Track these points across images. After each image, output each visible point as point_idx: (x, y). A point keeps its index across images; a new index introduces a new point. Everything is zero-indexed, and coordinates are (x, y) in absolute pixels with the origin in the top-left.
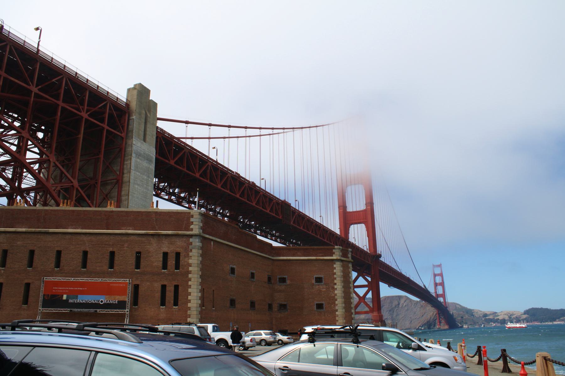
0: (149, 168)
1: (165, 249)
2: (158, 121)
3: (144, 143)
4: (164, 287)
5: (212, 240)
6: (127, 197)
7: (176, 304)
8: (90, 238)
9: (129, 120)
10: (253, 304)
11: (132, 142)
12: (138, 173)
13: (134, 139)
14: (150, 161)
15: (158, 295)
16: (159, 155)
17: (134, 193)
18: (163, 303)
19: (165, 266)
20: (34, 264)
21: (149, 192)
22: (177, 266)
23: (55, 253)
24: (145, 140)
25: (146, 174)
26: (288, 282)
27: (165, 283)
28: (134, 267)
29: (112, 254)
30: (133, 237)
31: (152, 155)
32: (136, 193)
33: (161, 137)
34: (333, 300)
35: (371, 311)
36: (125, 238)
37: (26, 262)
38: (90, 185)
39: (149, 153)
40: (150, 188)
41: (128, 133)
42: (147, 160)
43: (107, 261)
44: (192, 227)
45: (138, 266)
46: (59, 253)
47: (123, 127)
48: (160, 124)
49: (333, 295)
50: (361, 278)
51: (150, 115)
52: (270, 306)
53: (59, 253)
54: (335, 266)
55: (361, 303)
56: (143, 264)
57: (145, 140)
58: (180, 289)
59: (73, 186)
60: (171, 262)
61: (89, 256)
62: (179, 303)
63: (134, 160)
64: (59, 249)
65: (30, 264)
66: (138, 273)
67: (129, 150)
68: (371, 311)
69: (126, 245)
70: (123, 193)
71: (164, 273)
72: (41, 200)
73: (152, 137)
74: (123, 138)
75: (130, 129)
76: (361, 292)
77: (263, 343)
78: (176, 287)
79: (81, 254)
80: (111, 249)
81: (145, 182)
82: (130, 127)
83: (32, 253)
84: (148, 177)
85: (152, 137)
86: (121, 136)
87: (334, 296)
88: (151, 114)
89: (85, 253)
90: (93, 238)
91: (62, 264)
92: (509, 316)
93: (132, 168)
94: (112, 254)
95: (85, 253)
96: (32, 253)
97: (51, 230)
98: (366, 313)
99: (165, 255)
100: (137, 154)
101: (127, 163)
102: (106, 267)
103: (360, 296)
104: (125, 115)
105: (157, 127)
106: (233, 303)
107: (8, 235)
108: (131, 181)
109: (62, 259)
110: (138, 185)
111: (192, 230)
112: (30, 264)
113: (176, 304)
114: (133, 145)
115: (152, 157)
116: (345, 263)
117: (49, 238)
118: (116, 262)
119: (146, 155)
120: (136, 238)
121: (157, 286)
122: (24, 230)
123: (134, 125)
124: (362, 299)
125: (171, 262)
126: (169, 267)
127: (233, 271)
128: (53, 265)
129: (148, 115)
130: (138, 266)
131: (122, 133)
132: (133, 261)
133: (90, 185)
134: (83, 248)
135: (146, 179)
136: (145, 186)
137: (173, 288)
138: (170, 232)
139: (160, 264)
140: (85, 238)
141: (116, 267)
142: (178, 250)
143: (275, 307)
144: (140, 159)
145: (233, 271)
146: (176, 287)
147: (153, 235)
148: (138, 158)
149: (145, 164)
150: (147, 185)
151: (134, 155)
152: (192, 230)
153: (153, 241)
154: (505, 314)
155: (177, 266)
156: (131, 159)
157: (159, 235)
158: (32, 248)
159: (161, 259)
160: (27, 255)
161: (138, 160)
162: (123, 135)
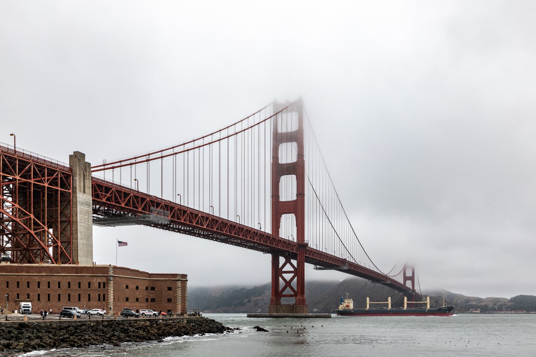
0: (89, 210)
1: (99, 281)
2: (93, 173)
3: (84, 194)
4: (99, 295)
5: (117, 277)
6: (76, 231)
7: (104, 301)
8: (70, 277)
9: (73, 180)
10: (137, 300)
11: (77, 196)
12: (82, 215)
13: (77, 193)
14: (89, 205)
15: (97, 298)
16: (95, 198)
17: (81, 229)
18: (99, 300)
19: (99, 287)
20: (50, 287)
21: (90, 226)
22: (104, 288)
23: (58, 283)
24: (84, 192)
25: (87, 215)
26: (156, 289)
27: (100, 293)
28: (88, 288)
29: (79, 283)
30: (86, 277)
31: (90, 201)
32: (82, 228)
33: (95, 184)
34: (176, 297)
35: (295, 295)
36: (84, 277)
37: (47, 286)
38: (51, 222)
39: (88, 201)
40: (90, 223)
41: (74, 192)
42: (87, 205)
43: (78, 286)
44: (109, 273)
45: (89, 287)
46: (59, 283)
47: (69, 185)
48: (94, 174)
49: (176, 295)
50: (288, 264)
51: (87, 173)
52: (147, 300)
53: (59, 283)
54: (177, 283)
55: (287, 287)
56: (91, 286)
57: (84, 192)
58: (105, 296)
59: (45, 230)
60: (102, 286)
61: (71, 284)
62: (105, 300)
63: (79, 208)
64: (59, 281)
65: (49, 287)
66: (90, 290)
67: (74, 200)
68: (295, 295)
69: (84, 280)
70: (74, 229)
71: (99, 290)
72: (24, 237)
73: (89, 189)
74: (70, 193)
75: (74, 186)
76: (288, 277)
77: (134, 316)
78: (104, 295)
79: (68, 283)
80: (79, 281)
81: (87, 220)
82: (74, 185)
83: (49, 283)
84: (89, 216)
85: (89, 189)
86: (69, 192)
87: (176, 296)
88: (87, 172)
89: (69, 283)
90: (72, 277)
91: (61, 287)
92: (493, 303)
93: (78, 213)
94: (79, 283)
95: (69, 283)
96: (49, 283)
97: (55, 274)
98: (291, 296)
99: (99, 283)
100: (80, 203)
101: (74, 209)
102: (77, 288)
103: (287, 281)
104: (70, 177)
105: (92, 177)
106: (127, 299)
107: (39, 276)
108: (78, 221)
109: (60, 285)
110: (83, 223)
111: (109, 274)
112: (49, 287)
113: (104, 301)
114: (77, 198)
115: (90, 203)
116: (182, 281)
117: (55, 277)
118: (81, 286)
119: (86, 202)
120: (88, 277)
121: (97, 295)
122: (45, 274)
123: (77, 184)
124: (288, 284)
125: (102, 286)
126: (101, 288)
127: (127, 287)
128: (57, 287)
129: (85, 174)
130: (89, 287)
131: (69, 190)
132: (87, 285)
133: (51, 222)
134: (68, 281)
135: (87, 218)
136: (87, 223)
137: (103, 295)
138: (101, 275)
139: (98, 286)
140: (69, 277)
141: (81, 288)
142: (104, 281)
143: (149, 300)
144: (83, 206)
145: (127, 287)
146: (104, 295)
147: (94, 276)
148: (81, 205)
149: (86, 208)
150: (88, 222)
151: (78, 204)
152: (109, 274)
153: (95, 278)
154: (490, 301)
155: (104, 288)
156: (77, 207)
157: (97, 276)
158: (49, 281)
159: (98, 285)
160: (47, 283)
161: (81, 207)
162: (71, 191)
